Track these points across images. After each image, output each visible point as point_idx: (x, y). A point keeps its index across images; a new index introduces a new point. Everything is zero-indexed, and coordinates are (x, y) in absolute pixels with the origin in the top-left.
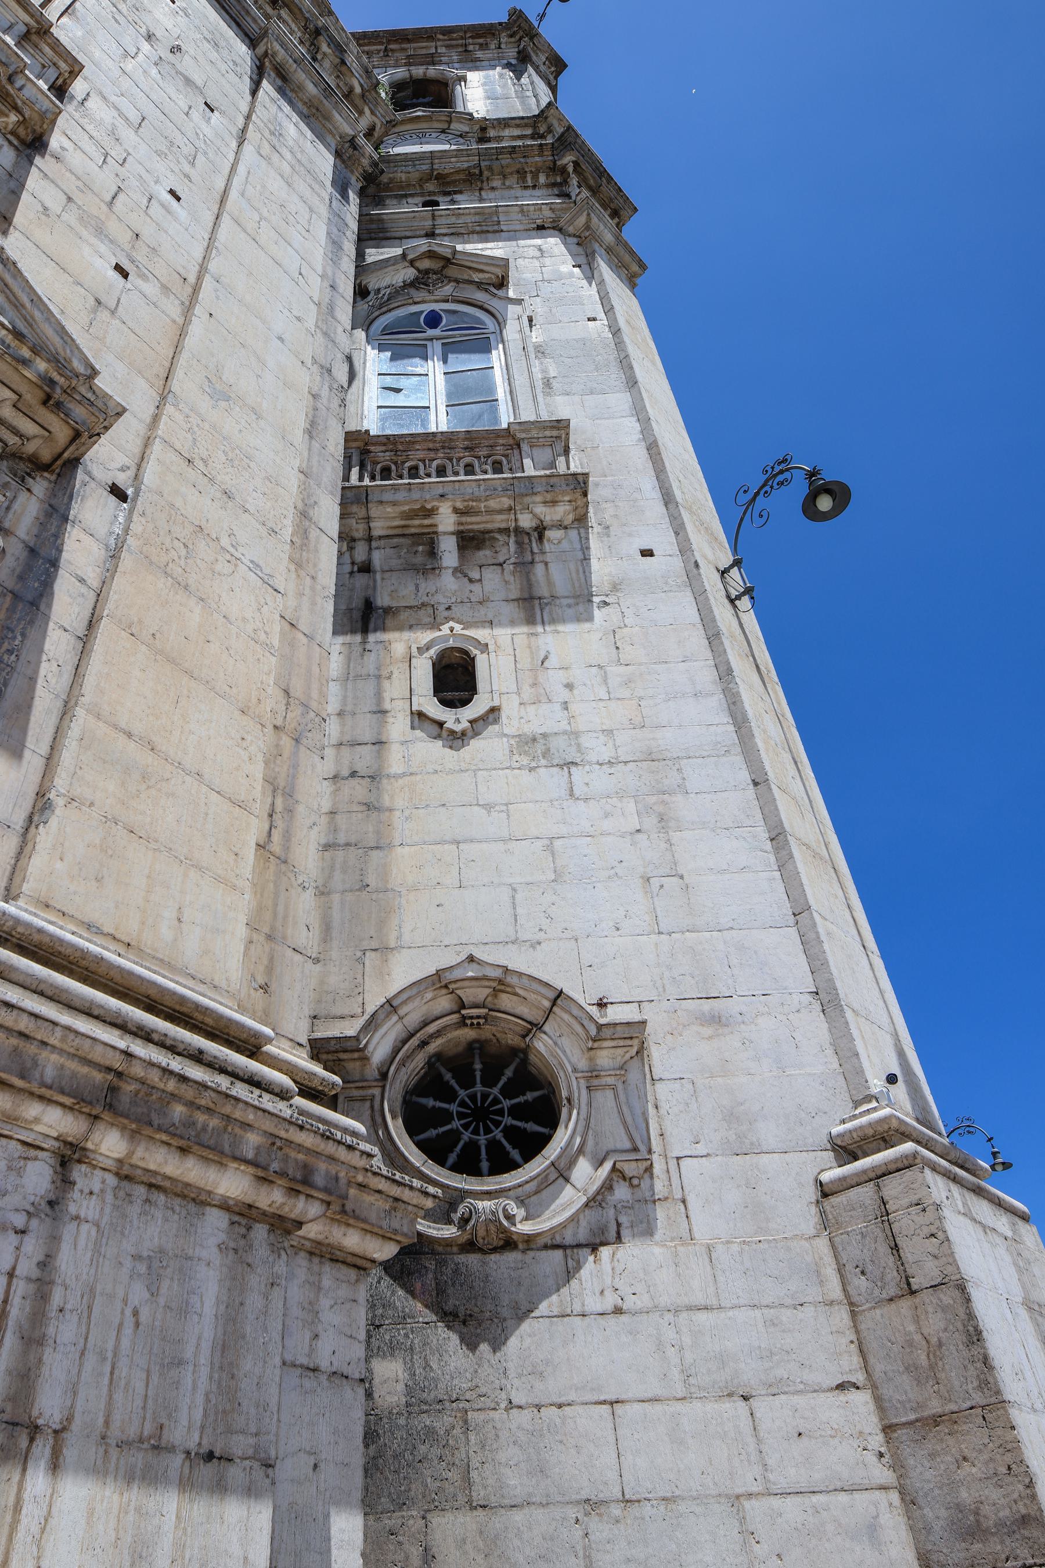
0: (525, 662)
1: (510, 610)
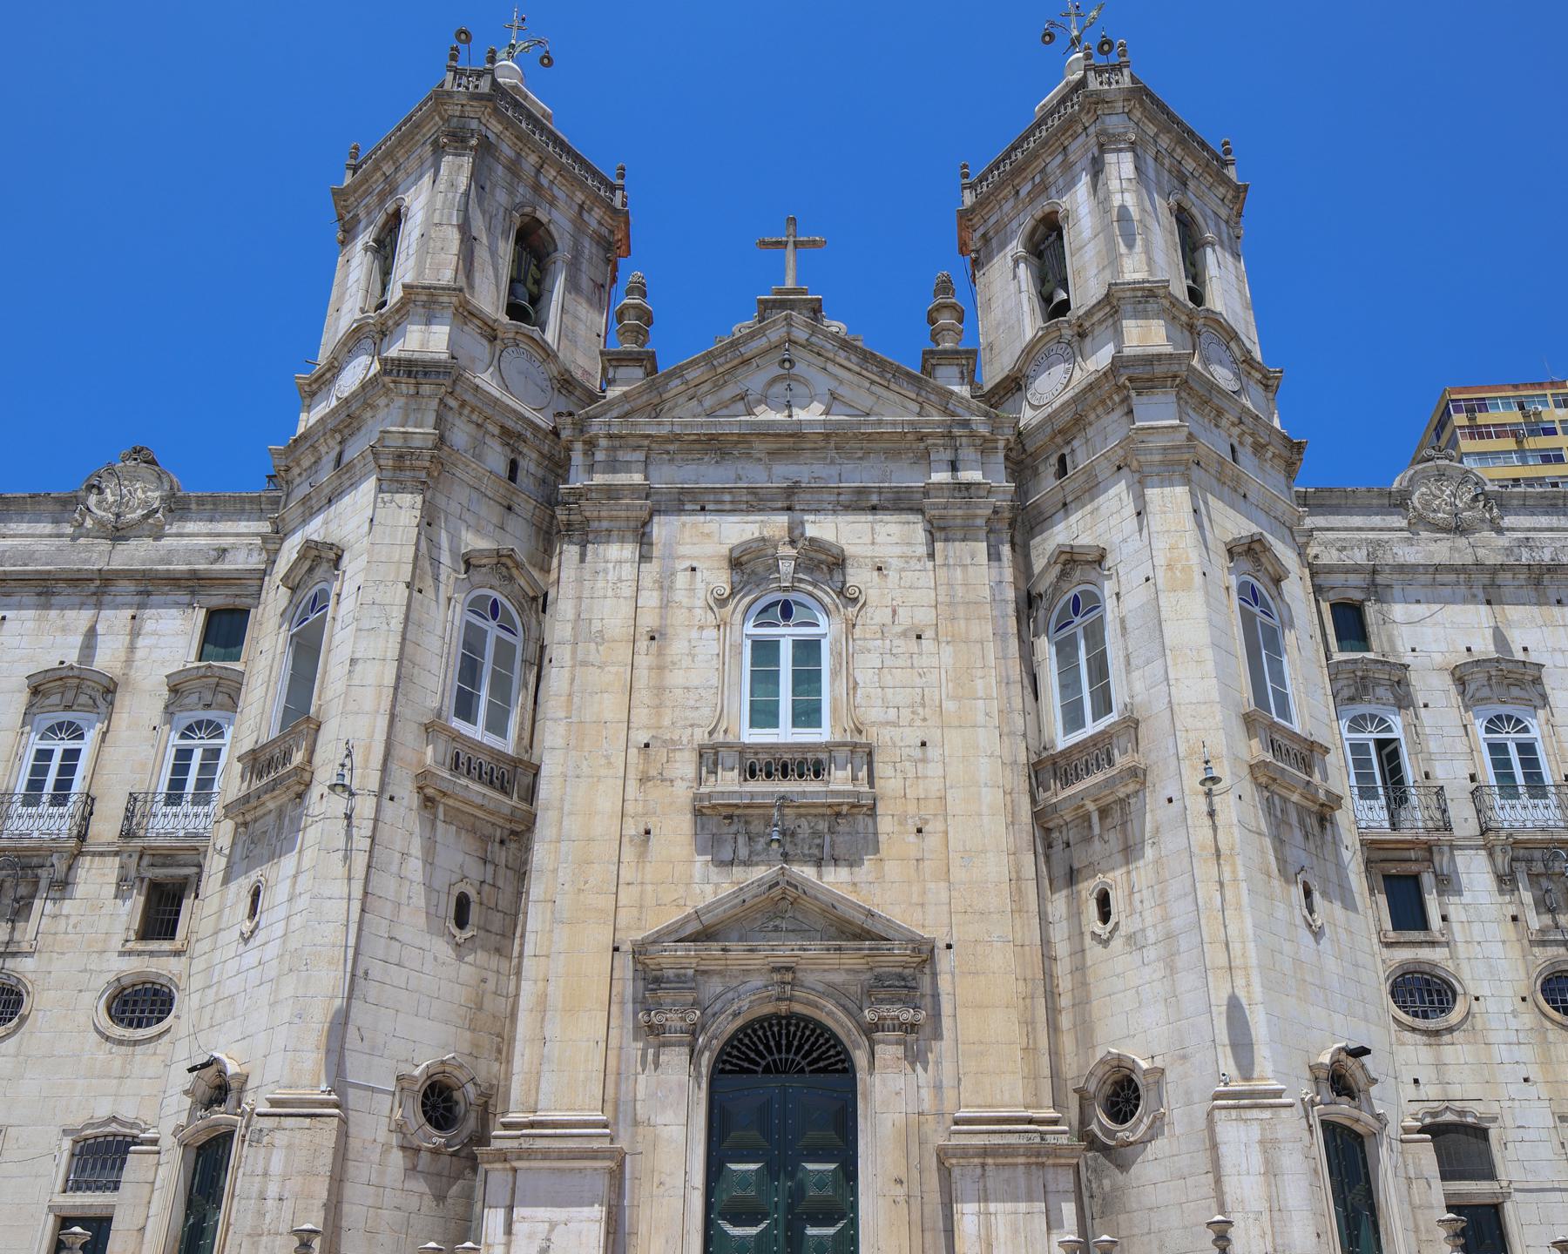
0: (1126, 893)
1: (1119, 857)
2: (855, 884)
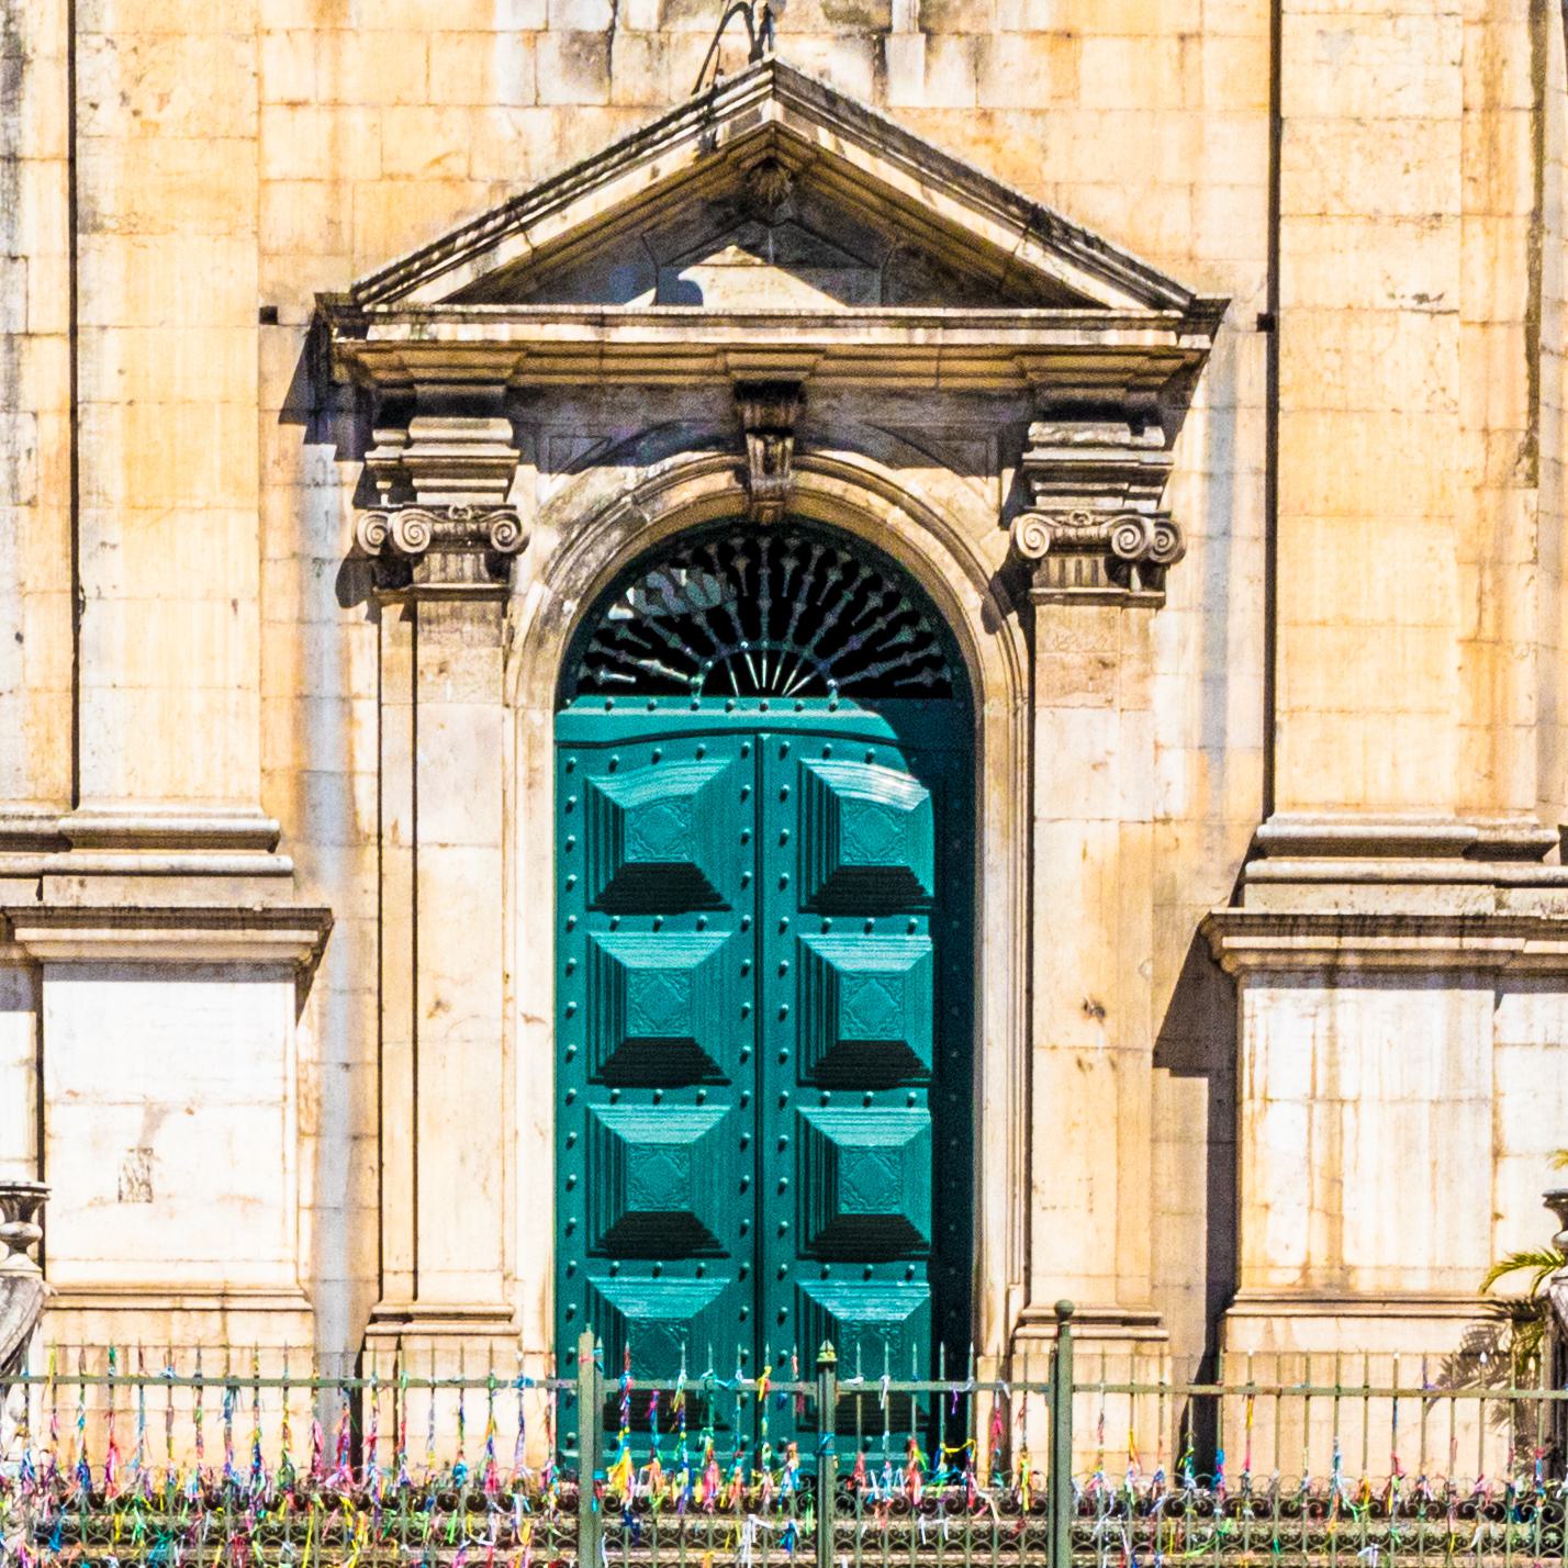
2: (986, 116)
